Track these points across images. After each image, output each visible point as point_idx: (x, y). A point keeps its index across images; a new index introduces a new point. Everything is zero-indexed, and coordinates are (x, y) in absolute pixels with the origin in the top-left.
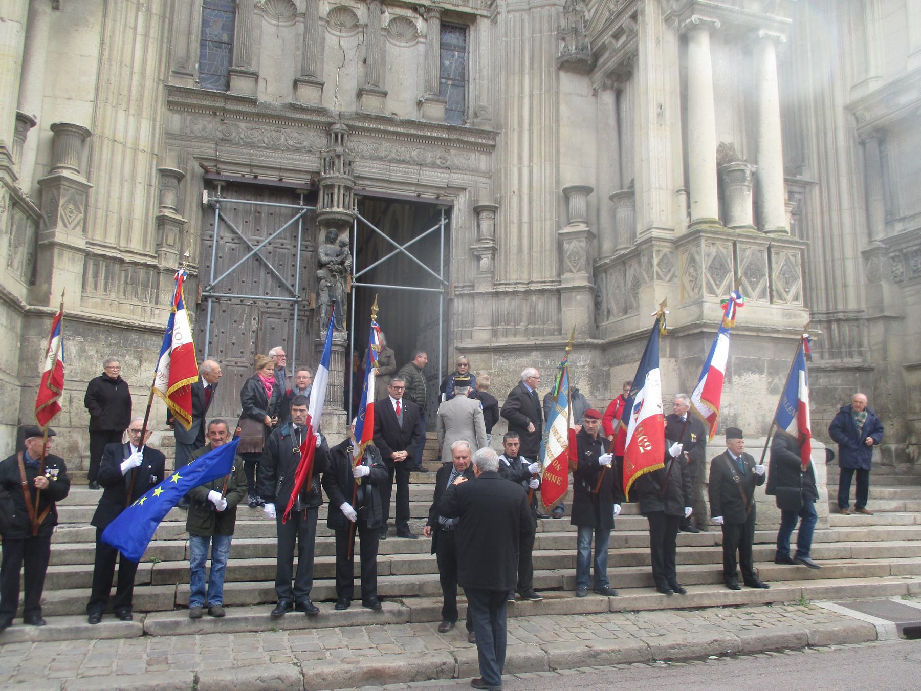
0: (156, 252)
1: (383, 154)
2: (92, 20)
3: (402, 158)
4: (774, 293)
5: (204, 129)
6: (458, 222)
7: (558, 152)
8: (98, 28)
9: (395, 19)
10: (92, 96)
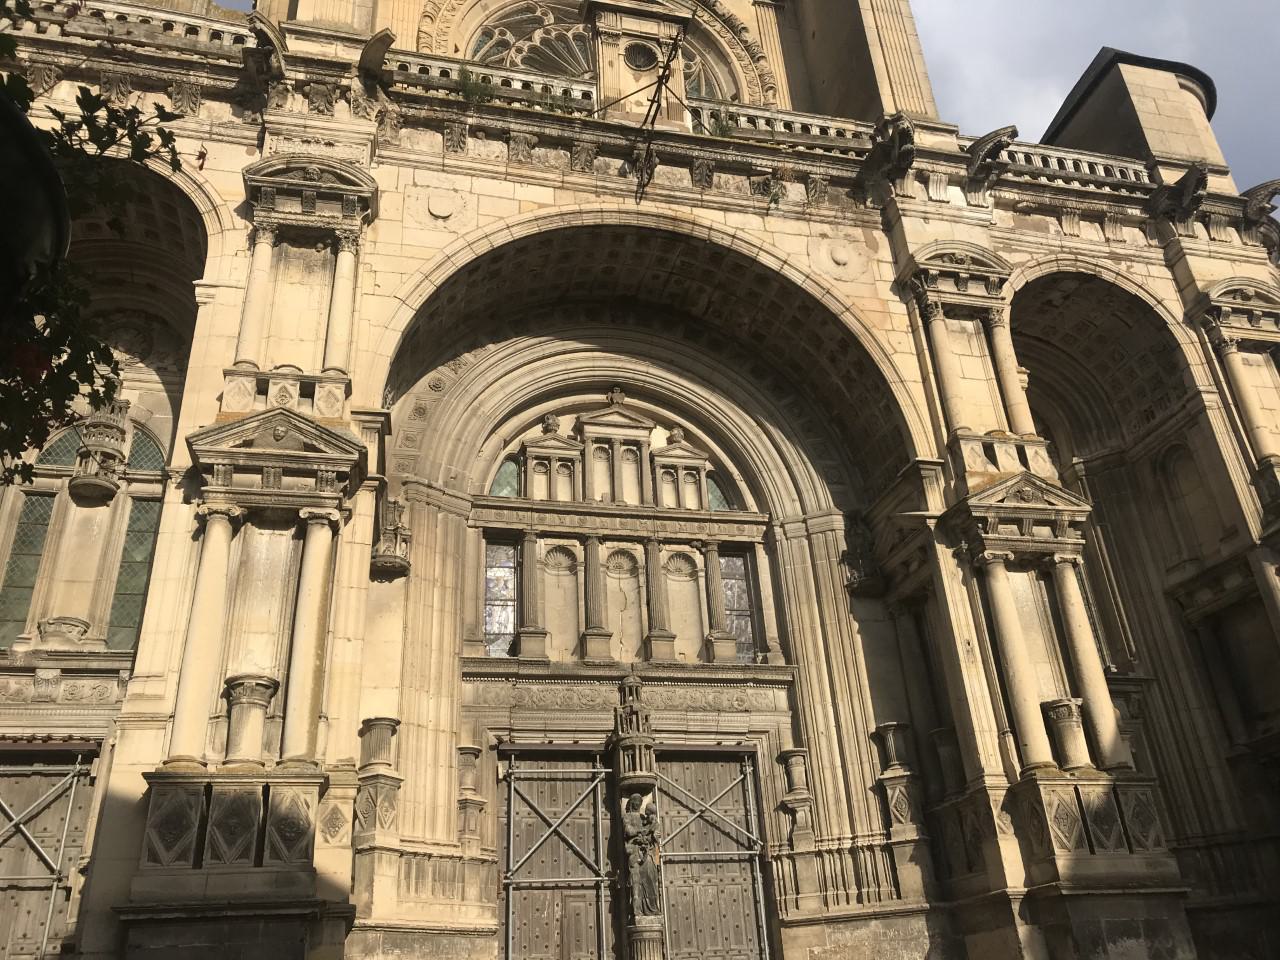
0: (459, 839)
1: (677, 702)
2: (394, 604)
3: (698, 704)
4: (1132, 840)
5: (497, 695)
6: (764, 769)
8: (400, 612)
9: (672, 557)
10: (397, 682)
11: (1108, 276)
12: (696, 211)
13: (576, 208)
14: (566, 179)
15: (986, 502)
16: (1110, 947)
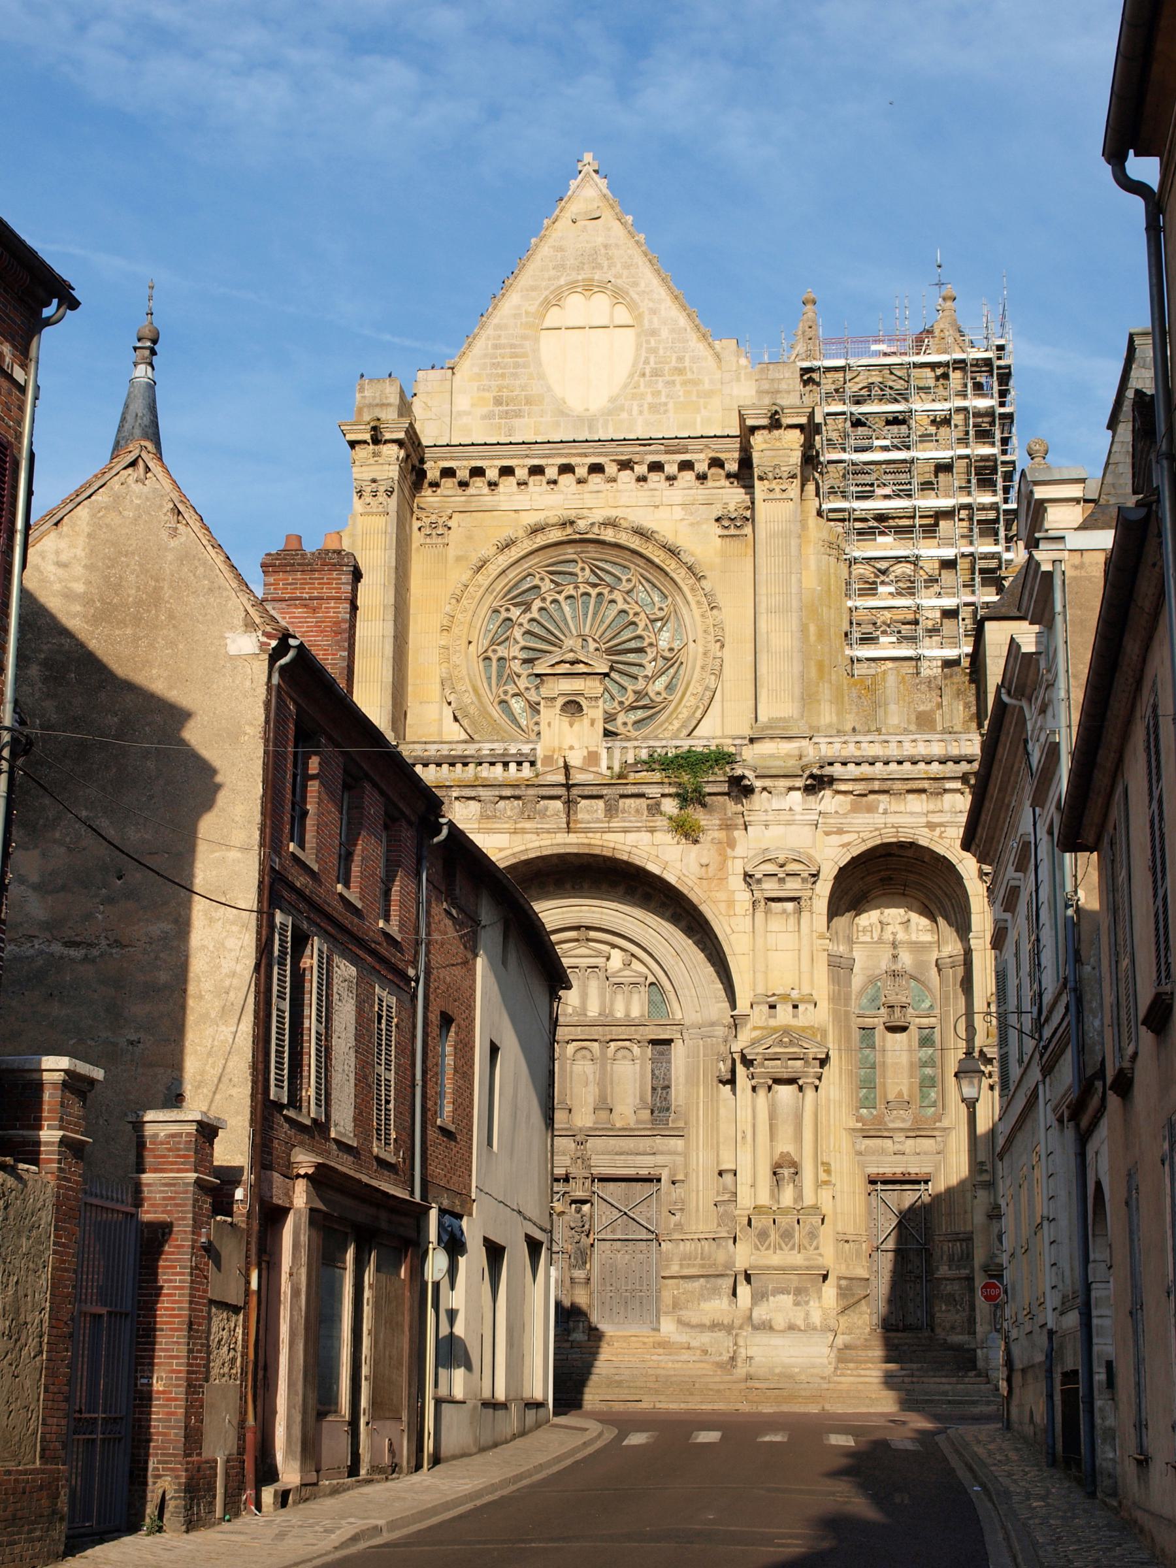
7: (718, 1143)
11: (923, 842)
12: (606, 836)
13: (523, 848)
14: (518, 826)
15: (756, 1051)
16: (771, 1298)
